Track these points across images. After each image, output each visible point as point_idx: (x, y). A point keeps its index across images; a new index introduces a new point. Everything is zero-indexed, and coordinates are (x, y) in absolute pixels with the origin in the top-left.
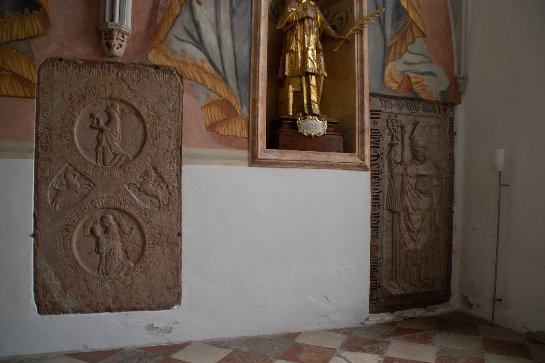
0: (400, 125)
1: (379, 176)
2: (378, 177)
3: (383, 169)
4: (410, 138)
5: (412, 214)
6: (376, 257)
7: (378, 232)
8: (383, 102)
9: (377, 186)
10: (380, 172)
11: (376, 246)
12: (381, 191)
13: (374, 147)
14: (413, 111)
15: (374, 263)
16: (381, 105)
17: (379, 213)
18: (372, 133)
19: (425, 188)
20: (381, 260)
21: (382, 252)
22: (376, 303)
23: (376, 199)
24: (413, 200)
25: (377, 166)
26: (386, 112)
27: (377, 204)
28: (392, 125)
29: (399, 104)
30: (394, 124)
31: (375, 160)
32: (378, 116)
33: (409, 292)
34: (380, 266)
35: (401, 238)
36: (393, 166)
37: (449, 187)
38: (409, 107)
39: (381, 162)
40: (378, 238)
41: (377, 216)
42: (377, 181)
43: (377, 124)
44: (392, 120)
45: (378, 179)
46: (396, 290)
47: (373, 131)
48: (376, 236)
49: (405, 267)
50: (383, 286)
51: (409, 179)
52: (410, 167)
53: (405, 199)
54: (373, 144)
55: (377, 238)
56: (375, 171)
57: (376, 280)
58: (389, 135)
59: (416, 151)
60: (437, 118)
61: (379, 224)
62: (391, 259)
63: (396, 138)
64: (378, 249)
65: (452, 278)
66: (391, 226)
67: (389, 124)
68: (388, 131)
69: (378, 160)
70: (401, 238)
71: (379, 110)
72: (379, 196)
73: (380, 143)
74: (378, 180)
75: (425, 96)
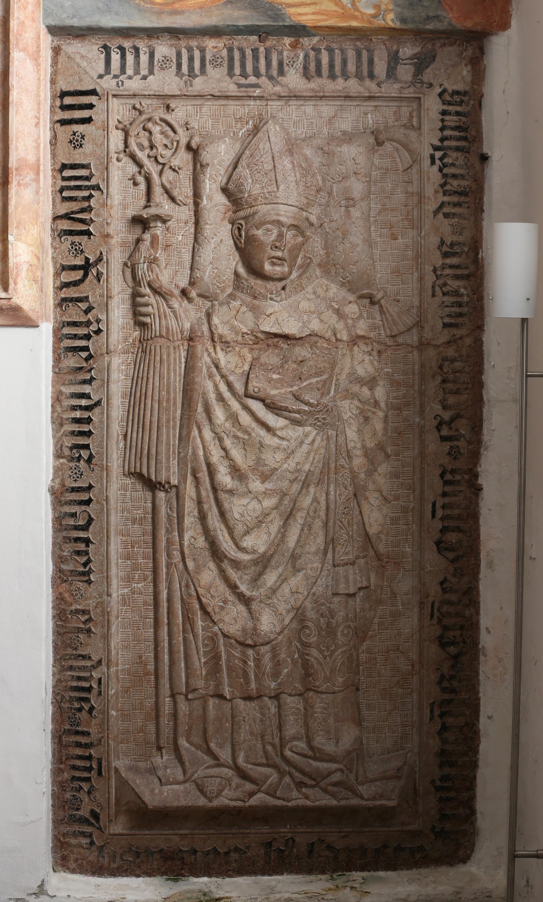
0: (184, 141)
1: (90, 344)
2: (86, 349)
3: (103, 317)
4: (225, 190)
5: (231, 492)
6: (84, 657)
7: (89, 561)
8: (115, 57)
9: (84, 382)
10: (94, 327)
11: (84, 612)
12: (98, 403)
13: (71, 233)
14: (252, 80)
15: (79, 679)
16: (102, 70)
17: (90, 487)
18: (64, 179)
19: (296, 388)
20: (104, 668)
21: (106, 637)
22: (90, 835)
23: (81, 434)
24: (236, 437)
25: (83, 306)
26: (114, 96)
27: (85, 454)
28: (146, 144)
29: (191, 59)
30: (158, 139)
31: (75, 284)
32: (85, 114)
33: (227, 801)
34: (100, 693)
35: (187, 586)
36: (147, 305)
37: (444, 381)
38: (237, 64)
39: (98, 291)
40: (89, 582)
41: (84, 497)
42: (84, 365)
43: (81, 146)
44: (150, 125)
45: (84, 354)
46: (166, 788)
47: (68, 173)
48: (83, 574)
49: (212, 702)
50: (116, 770)
51: (221, 355)
52: (228, 303)
53: (200, 431)
54: (69, 222)
55: (86, 585)
56: (74, 324)
57: (87, 746)
58: (135, 184)
59: (251, 240)
60: (370, 98)
61: (91, 528)
62: (151, 667)
63: (167, 192)
64: (91, 625)
65: (481, 763)
66: (149, 538)
67: (132, 141)
68: (132, 169)
69: (87, 281)
70: (187, 586)
71: (91, 87)
72: (89, 420)
73: (92, 215)
74: (87, 360)
75: (313, 13)
